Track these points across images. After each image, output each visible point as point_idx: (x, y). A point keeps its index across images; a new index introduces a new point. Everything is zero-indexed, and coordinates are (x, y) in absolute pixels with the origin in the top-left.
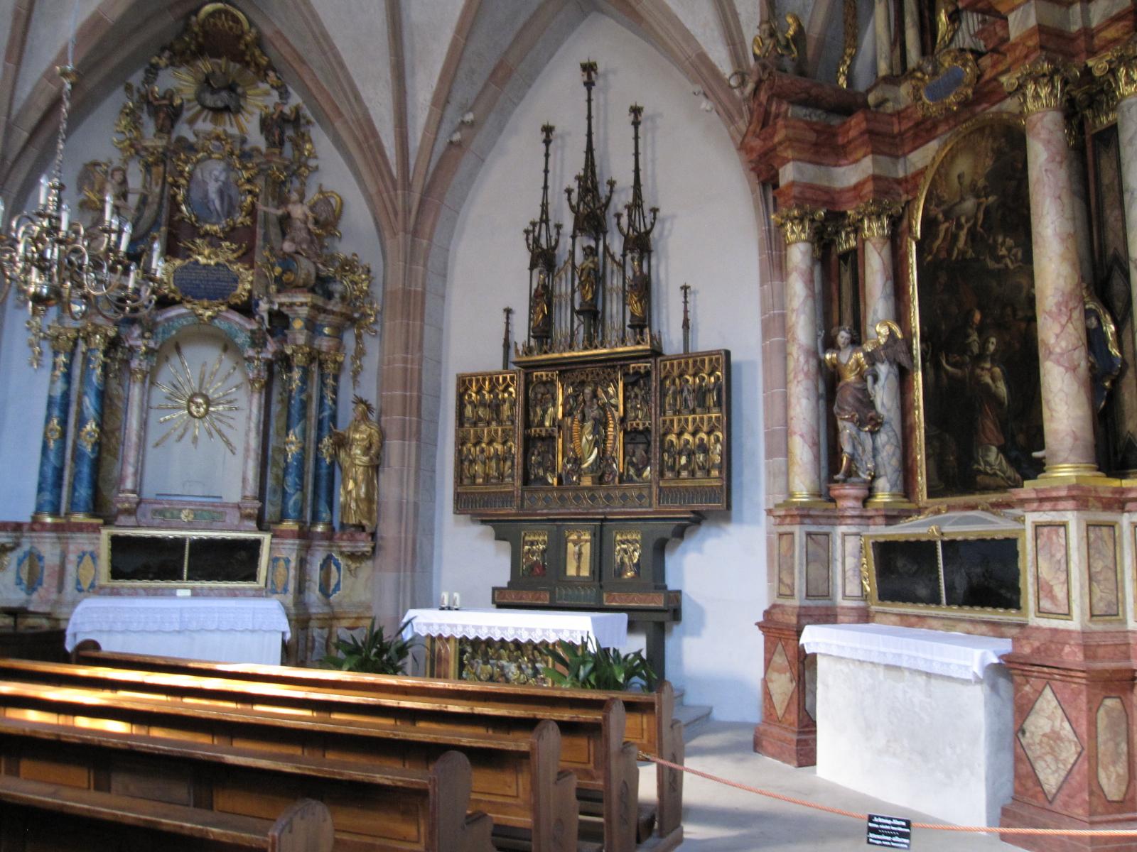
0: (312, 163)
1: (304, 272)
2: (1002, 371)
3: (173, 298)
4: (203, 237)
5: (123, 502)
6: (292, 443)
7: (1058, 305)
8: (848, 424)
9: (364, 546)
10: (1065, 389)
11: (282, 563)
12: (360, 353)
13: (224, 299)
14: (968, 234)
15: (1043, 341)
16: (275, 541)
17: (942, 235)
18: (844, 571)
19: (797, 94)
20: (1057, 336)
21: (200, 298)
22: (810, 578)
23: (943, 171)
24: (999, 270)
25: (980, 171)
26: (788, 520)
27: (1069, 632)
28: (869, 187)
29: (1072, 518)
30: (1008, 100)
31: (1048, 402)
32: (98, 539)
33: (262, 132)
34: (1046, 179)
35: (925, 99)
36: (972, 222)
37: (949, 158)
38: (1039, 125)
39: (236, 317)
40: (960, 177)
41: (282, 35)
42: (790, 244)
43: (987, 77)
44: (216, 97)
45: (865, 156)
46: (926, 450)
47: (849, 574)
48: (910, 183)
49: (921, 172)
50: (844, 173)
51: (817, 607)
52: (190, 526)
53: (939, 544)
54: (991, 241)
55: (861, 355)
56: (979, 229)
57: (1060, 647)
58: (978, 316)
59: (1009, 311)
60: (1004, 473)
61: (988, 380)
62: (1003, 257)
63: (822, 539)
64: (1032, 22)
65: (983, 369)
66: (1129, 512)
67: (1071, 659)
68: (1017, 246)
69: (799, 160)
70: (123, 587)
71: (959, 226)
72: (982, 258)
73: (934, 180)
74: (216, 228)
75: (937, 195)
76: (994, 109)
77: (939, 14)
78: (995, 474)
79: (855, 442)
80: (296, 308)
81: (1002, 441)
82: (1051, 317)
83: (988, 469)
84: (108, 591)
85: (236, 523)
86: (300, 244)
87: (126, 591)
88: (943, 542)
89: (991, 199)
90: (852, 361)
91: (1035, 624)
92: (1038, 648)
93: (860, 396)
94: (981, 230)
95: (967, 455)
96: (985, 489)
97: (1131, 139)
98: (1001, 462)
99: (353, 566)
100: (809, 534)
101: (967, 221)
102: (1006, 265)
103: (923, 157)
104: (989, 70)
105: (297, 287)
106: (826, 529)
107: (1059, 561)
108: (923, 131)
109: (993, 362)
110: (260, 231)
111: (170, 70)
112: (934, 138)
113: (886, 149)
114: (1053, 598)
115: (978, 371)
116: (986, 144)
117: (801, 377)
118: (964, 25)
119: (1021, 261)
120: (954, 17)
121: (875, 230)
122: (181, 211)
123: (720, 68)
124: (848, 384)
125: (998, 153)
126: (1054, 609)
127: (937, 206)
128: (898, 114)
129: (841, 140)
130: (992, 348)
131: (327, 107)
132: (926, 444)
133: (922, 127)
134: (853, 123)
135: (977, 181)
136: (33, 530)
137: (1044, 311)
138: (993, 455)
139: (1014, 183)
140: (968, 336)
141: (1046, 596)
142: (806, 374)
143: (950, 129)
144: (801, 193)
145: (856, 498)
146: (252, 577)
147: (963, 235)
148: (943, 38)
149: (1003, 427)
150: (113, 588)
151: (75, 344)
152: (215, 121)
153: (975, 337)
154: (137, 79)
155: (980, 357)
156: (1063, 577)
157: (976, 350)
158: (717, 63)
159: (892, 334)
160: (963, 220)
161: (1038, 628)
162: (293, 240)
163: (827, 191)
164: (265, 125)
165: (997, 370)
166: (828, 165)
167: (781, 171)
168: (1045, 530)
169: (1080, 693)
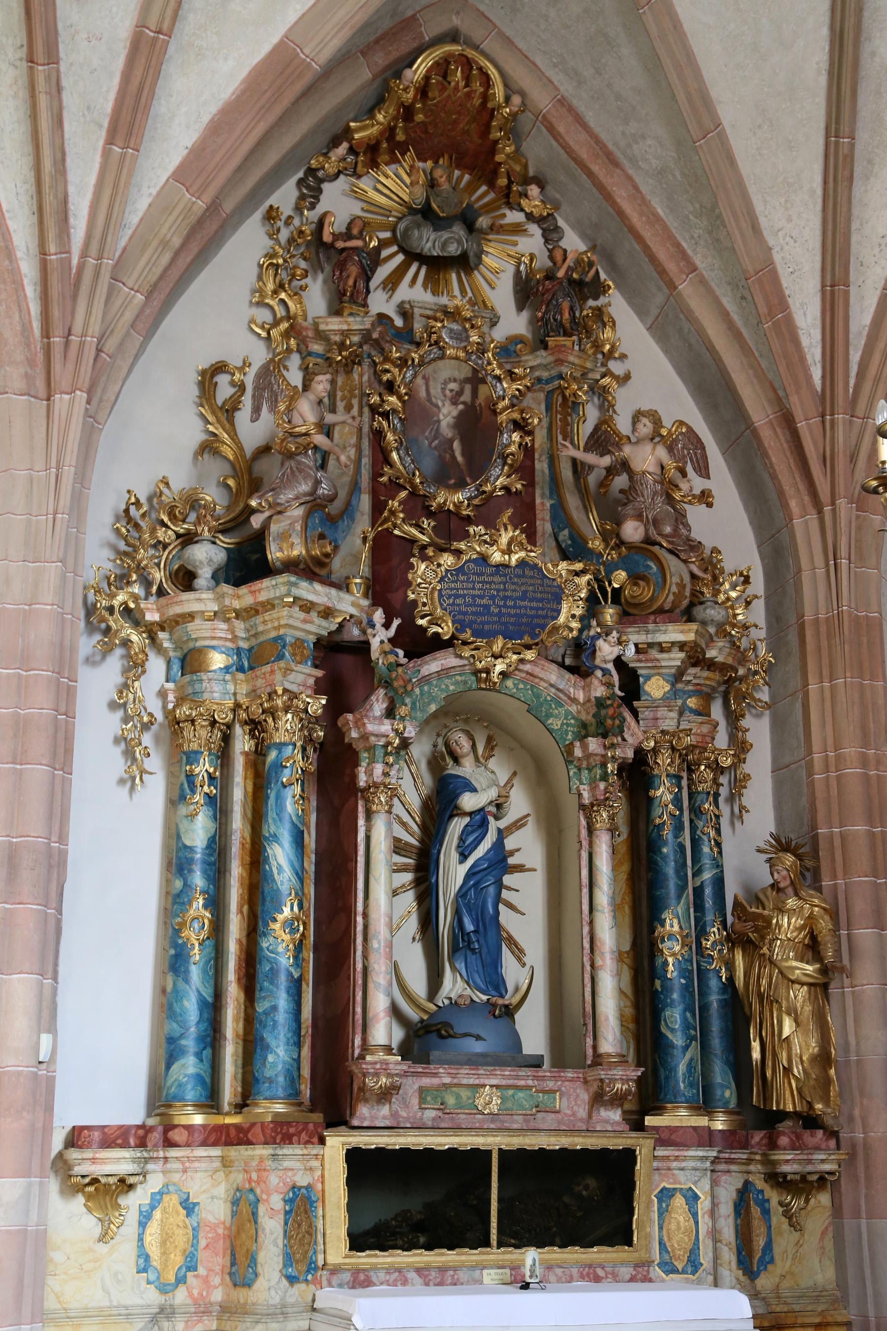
0: (616, 367)
1: (676, 579)
3: (436, 634)
4: (430, 514)
5: (377, 1075)
6: (671, 936)
9: (825, 1161)
11: (679, 1201)
12: (740, 747)
13: (533, 636)
16: (661, 1152)
21: (490, 636)
33: (520, 308)
39: (553, 675)
41: (571, 109)
44: (445, 235)
52: (497, 1122)
70: (375, 1268)
74: (459, 496)
80: (654, 653)
84: (347, 1277)
85: (582, 1113)
86: (656, 523)
87: (382, 1275)
99: (796, 1204)
105: (661, 611)
110: (543, 503)
111: (342, 182)
122: (391, 465)
131: (662, 254)
136: (169, 1143)
146: (622, 1236)
150: (356, 1271)
151: (227, 739)
152: (434, 283)
154: (285, 196)
162: (639, 517)
164: (526, 291)
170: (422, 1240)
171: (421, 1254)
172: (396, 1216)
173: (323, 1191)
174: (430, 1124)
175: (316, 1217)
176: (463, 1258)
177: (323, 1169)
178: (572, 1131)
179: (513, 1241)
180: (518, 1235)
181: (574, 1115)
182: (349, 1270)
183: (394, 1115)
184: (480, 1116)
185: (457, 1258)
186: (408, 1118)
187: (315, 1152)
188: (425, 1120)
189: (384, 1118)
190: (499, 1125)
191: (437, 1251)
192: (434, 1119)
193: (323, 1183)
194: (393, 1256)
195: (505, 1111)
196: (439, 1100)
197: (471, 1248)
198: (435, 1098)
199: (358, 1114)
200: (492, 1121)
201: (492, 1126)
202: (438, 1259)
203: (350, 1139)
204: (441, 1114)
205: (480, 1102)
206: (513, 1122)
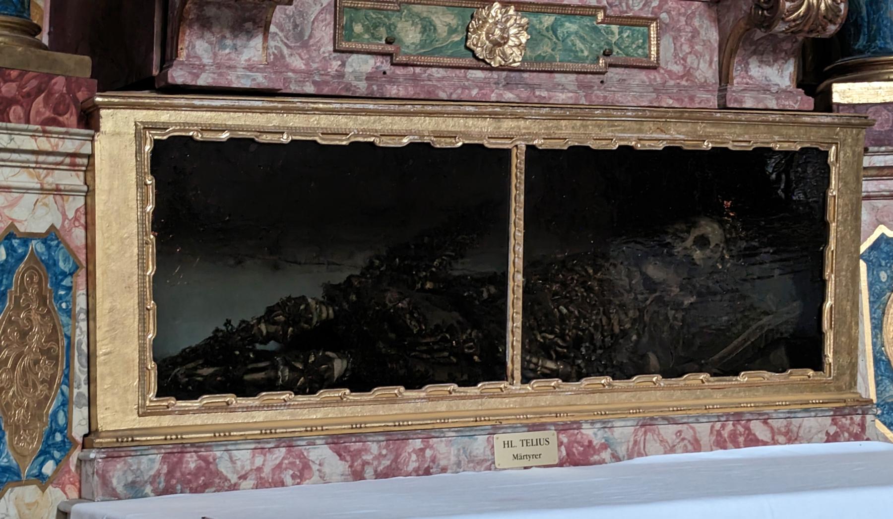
32: (86, 164)
85: (706, 70)
146: (801, 348)
170: (339, 366)
171: (340, 401)
172: (270, 310)
173: (90, 247)
174: (362, 87)
175: (70, 313)
176: (442, 406)
177: (90, 193)
178: (683, 114)
179: (551, 365)
180: (575, 348)
181: (688, 74)
182: (157, 446)
183: (277, 63)
184: (479, 74)
185: (429, 406)
186: (309, 73)
187: (69, 146)
188: (349, 78)
189: (250, 68)
190: (524, 94)
191: (379, 392)
192: (370, 78)
193: (89, 227)
194: (270, 407)
195: (538, 65)
196: (383, 32)
197: (408, 387)
198: (372, 28)
199: (183, 56)
200: (508, 85)
201: (509, 96)
202: (382, 411)
203: (164, 116)
204: (387, 67)
205: (479, 41)
206: (556, 87)
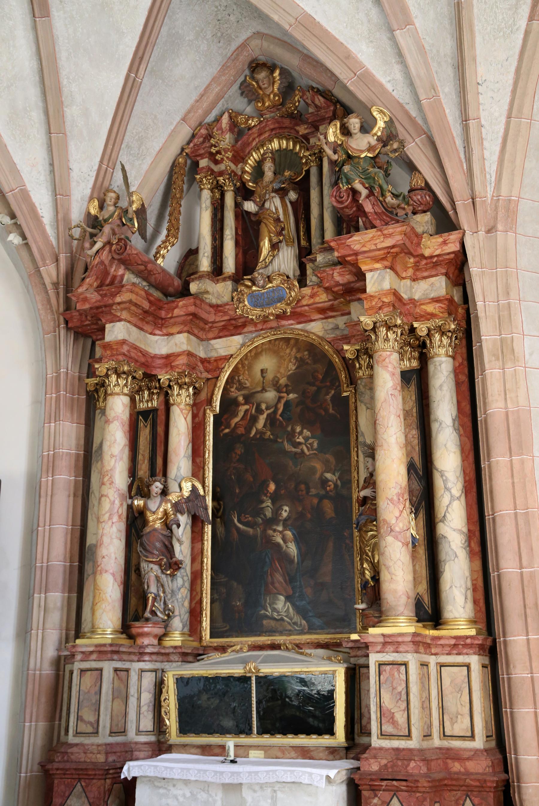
2: (293, 534)
7: (398, 495)
8: (156, 567)
10: (402, 559)
14: (267, 419)
15: (384, 520)
17: (241, 414)
18: (139, 706)
19: (138, 264)
20: (397, 518)
22: (114, 713)
23: (246, 362)
24: (296, 453)
25: (282, 370)
26: (94, 656)
27: (410, 750)
28: (182, 360)
29: (412, 659)
30: (313, 324)
31: (388, 568)
34: (391, 401)
35: (246, 303)
36: (272, 410)
37: (253, 354)
38: (387, 360)
40: (262, 371)
42: (111, 394)
43: (304, 302)
45: (179, 333)
46: (212, 594)
47: (144, 709)
48: (214, 365)
49: (227, 358)
50: (157, 342)
51: (117, 744)
53: (254, 679)
54: (289, 429)
55: (169, 505)
56: (278, 416)
57: (406, 762)
58: (272, 487)
59: (303, 487)
60: (291, 619)
61: (279, 540)
62: (300, 443)
63: (123, 674)
64: (386, 285)
65: (275, 531)
66: (436, 654)
67: (416, 771)
68: (312, 437)
69: (129, 322)
71: (259, 411)
72: (279, 440)
73: (236, 367)
75: (239, 381)
76: (299, 326)
77: (263, 239)
78: (282, 620)
79: (161, 585)
81: (291, 592)
82: (393, 504)
83: (275, 615)
88: (257, 678)
89: (292, 396)
90: (161, 510)
91: (377, 746)
92: (386, 765)
93: (167, 543)
94: (280, 418)
95: (254, 601)
96: (271, 632)
97: (441, 386)
98: (288, 608)
100: (116, 670)
101: (267, 408)
102: (302, 450)
103: (229, 346)
104: (307, 297)
106: (126, 665)
107: (400, 693)
108: (234, 326)
109: (285, 527)
112: (240, 334)
113: (196, 331)
114: (393, 721)
115: (270, 532)
116: (290, 352)
117: (115, 519)
118: (280, 254)
119: (316, 450)
120: (274, 247)
121: (182, 399)
123: (40, 211)
124: (155, 530)
125: (301, 362)
126: (395, 732)
127: (238, 389)
128: (217, 307)
129: (163, 314)
130: (285, 514)
132: (211, 589)
133: (233, 322)
134: (181, 303)
135: (279, 380)
137: (387, 498)
138: (281, 603)
139: (315, 388)
140: (263, 502)
141: (388, 722)
142: (120, 516)
143: (256, 331)
144: (128, 351)
145: (155, 636)
147: (262, 419)
148: (265, 260)
149: (291, 580)
153: (269, 503)
155: (275, 520)
156: (404, 705)
157: (269, 513)
158: (37, 205)
159: (194, 489)
160: (263, 406)
161: (381, 749)
163: (144, 354)
165: (289, 534)
166: (146, 332)
167: (108, 326)
168: (388, 668)
169: (425, 799)
